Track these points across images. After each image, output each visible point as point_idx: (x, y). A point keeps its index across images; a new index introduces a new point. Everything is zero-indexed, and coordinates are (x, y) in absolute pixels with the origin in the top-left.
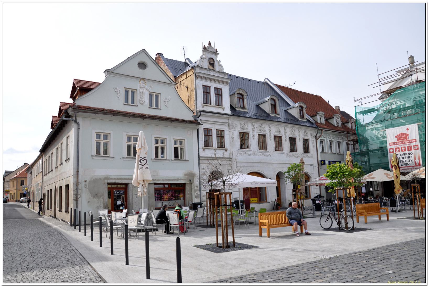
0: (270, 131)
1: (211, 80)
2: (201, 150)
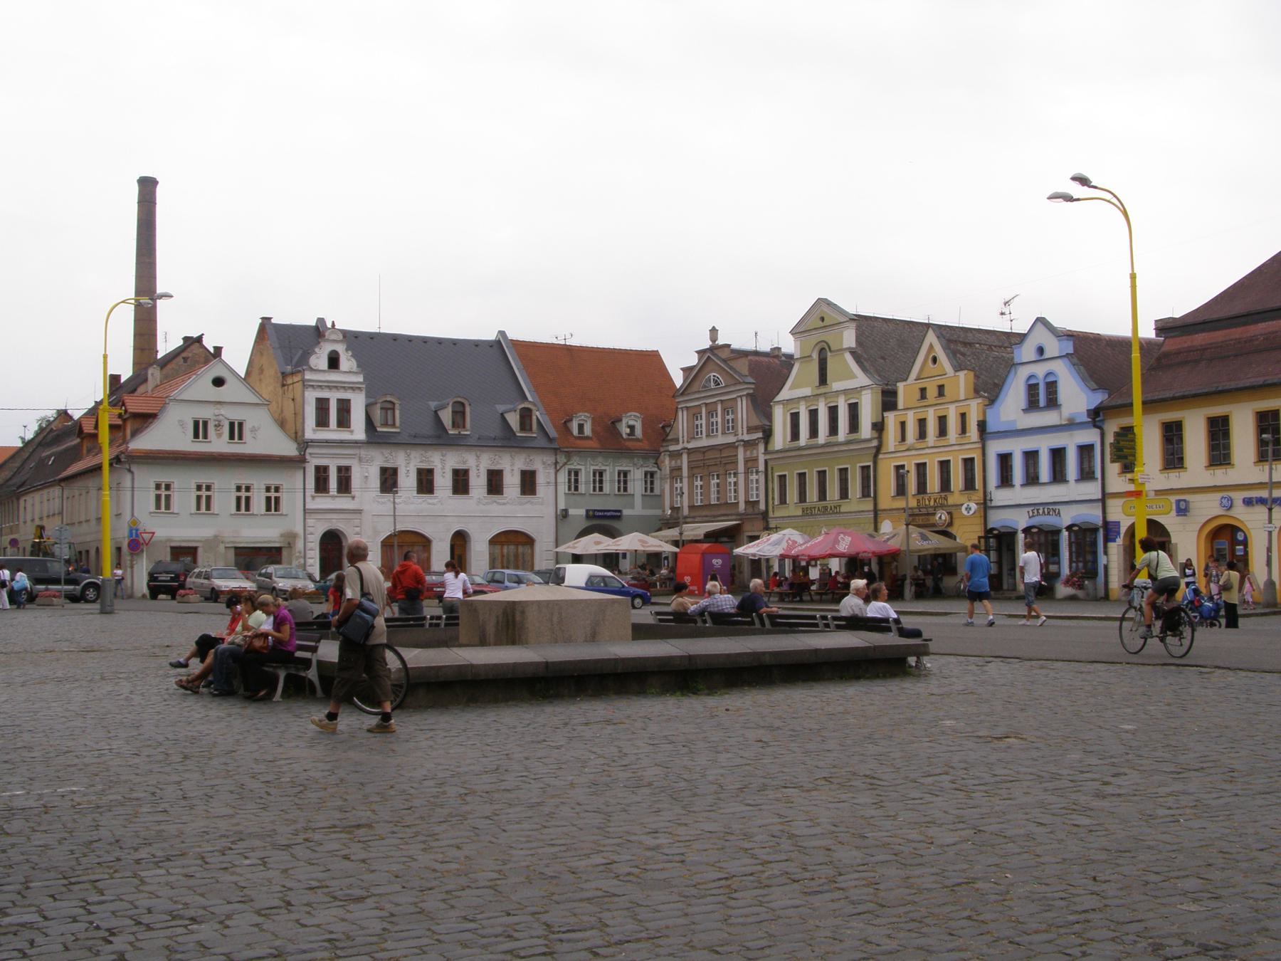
0: (443, 461)
2: (308, 499)
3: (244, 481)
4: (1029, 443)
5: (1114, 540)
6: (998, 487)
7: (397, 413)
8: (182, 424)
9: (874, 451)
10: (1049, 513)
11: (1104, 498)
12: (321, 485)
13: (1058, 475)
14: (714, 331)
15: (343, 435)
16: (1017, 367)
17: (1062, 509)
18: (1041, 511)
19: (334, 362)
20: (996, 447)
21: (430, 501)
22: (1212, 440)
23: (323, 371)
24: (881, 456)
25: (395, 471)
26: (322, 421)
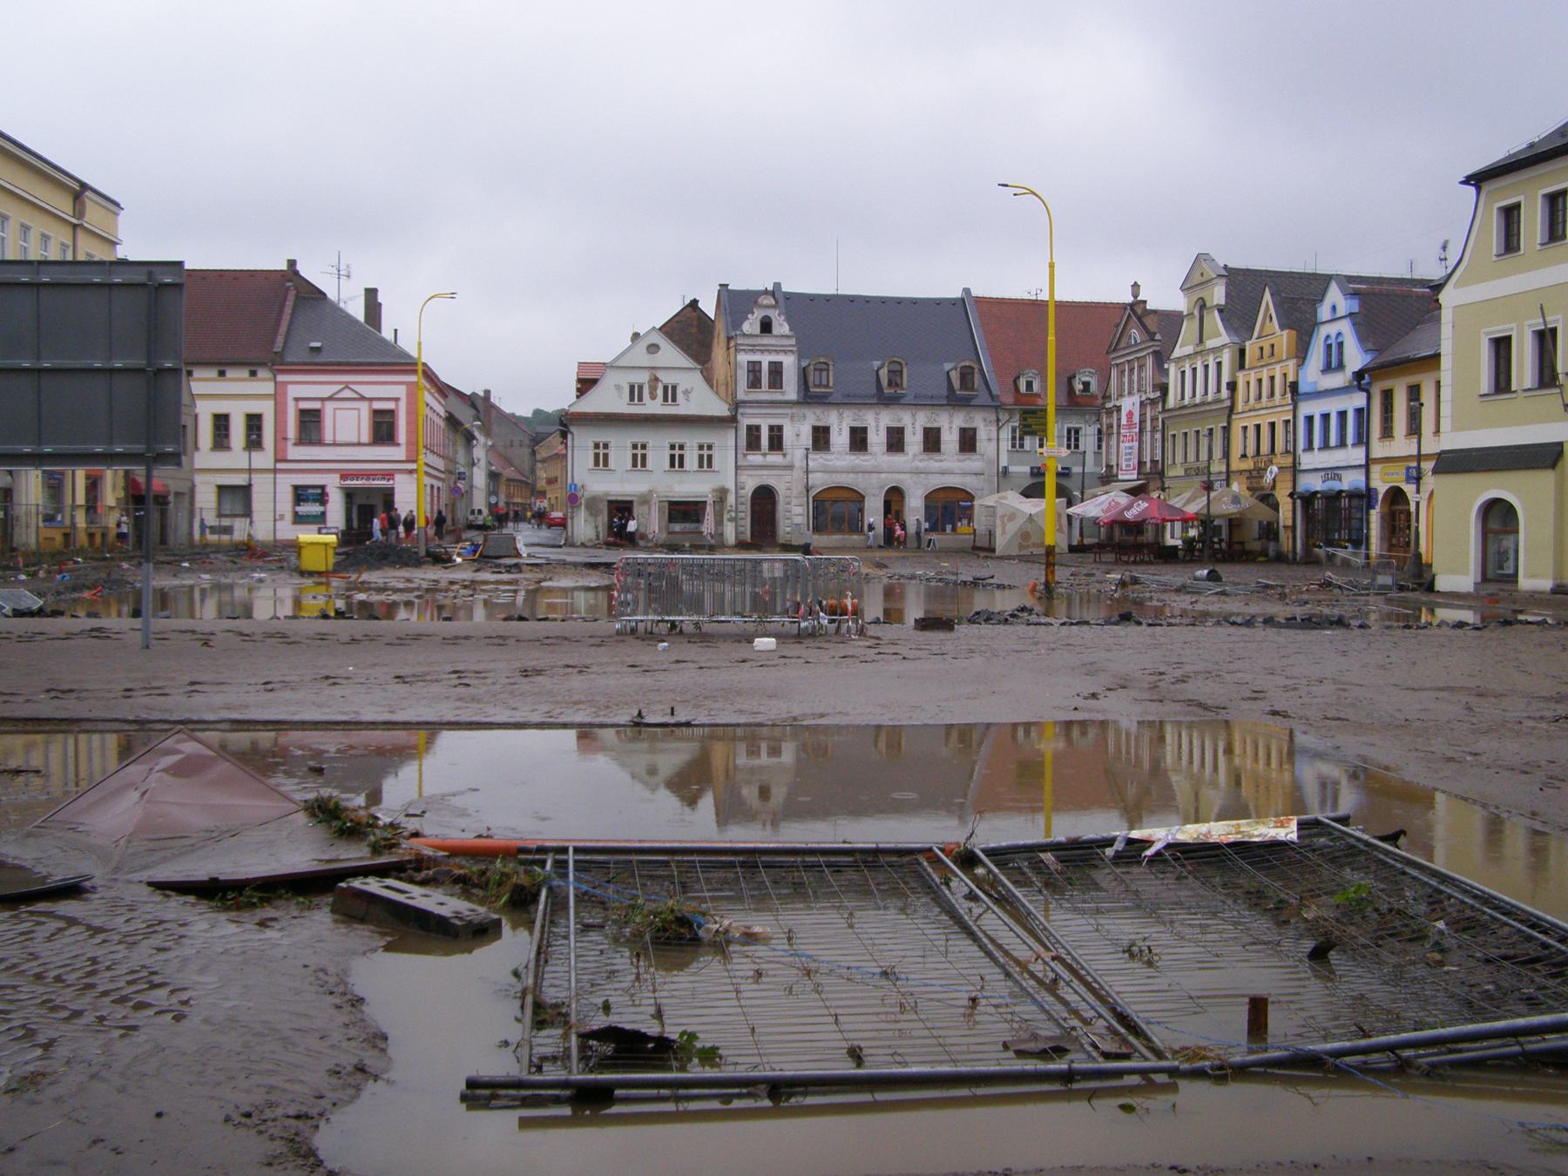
0: (877, 420)
1: (762, 352)
3: (677, 441)
5: (1374, 508)
6: (1304, 450)
7: (831, 373)
8: (618, 388)
9: (1227, 412)
12: (753, 443)
14: (1136, 286)
15: (776, 396)
17: (1343, 473)
19: (766, 327)
20: (1305, 409)
21: (862, 458)
23: (756, 336)
24: (1234, 417)
25: (826, 430)
26: (755, 383)
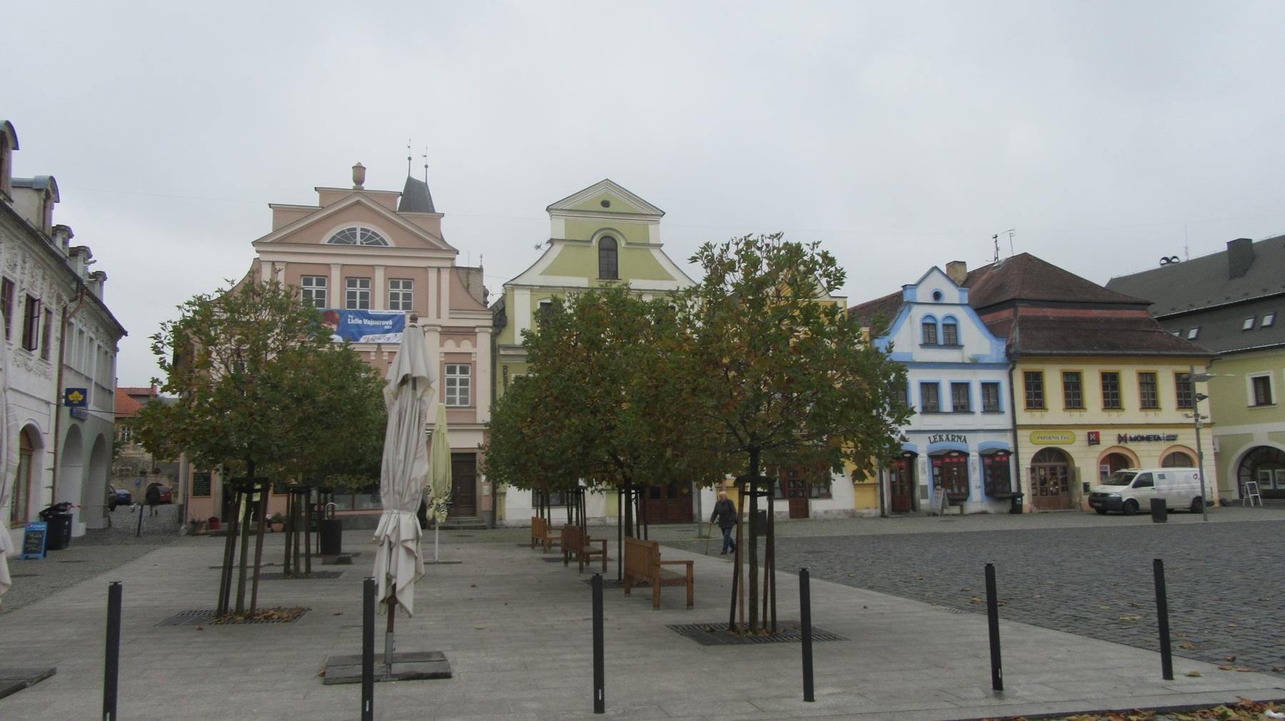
4: (929, 376)
10: (953, 440)
11: (1015, 428)
13: (962, 407)
16: (912, 305)
18: (944, 437)
22: (1117, 393)
